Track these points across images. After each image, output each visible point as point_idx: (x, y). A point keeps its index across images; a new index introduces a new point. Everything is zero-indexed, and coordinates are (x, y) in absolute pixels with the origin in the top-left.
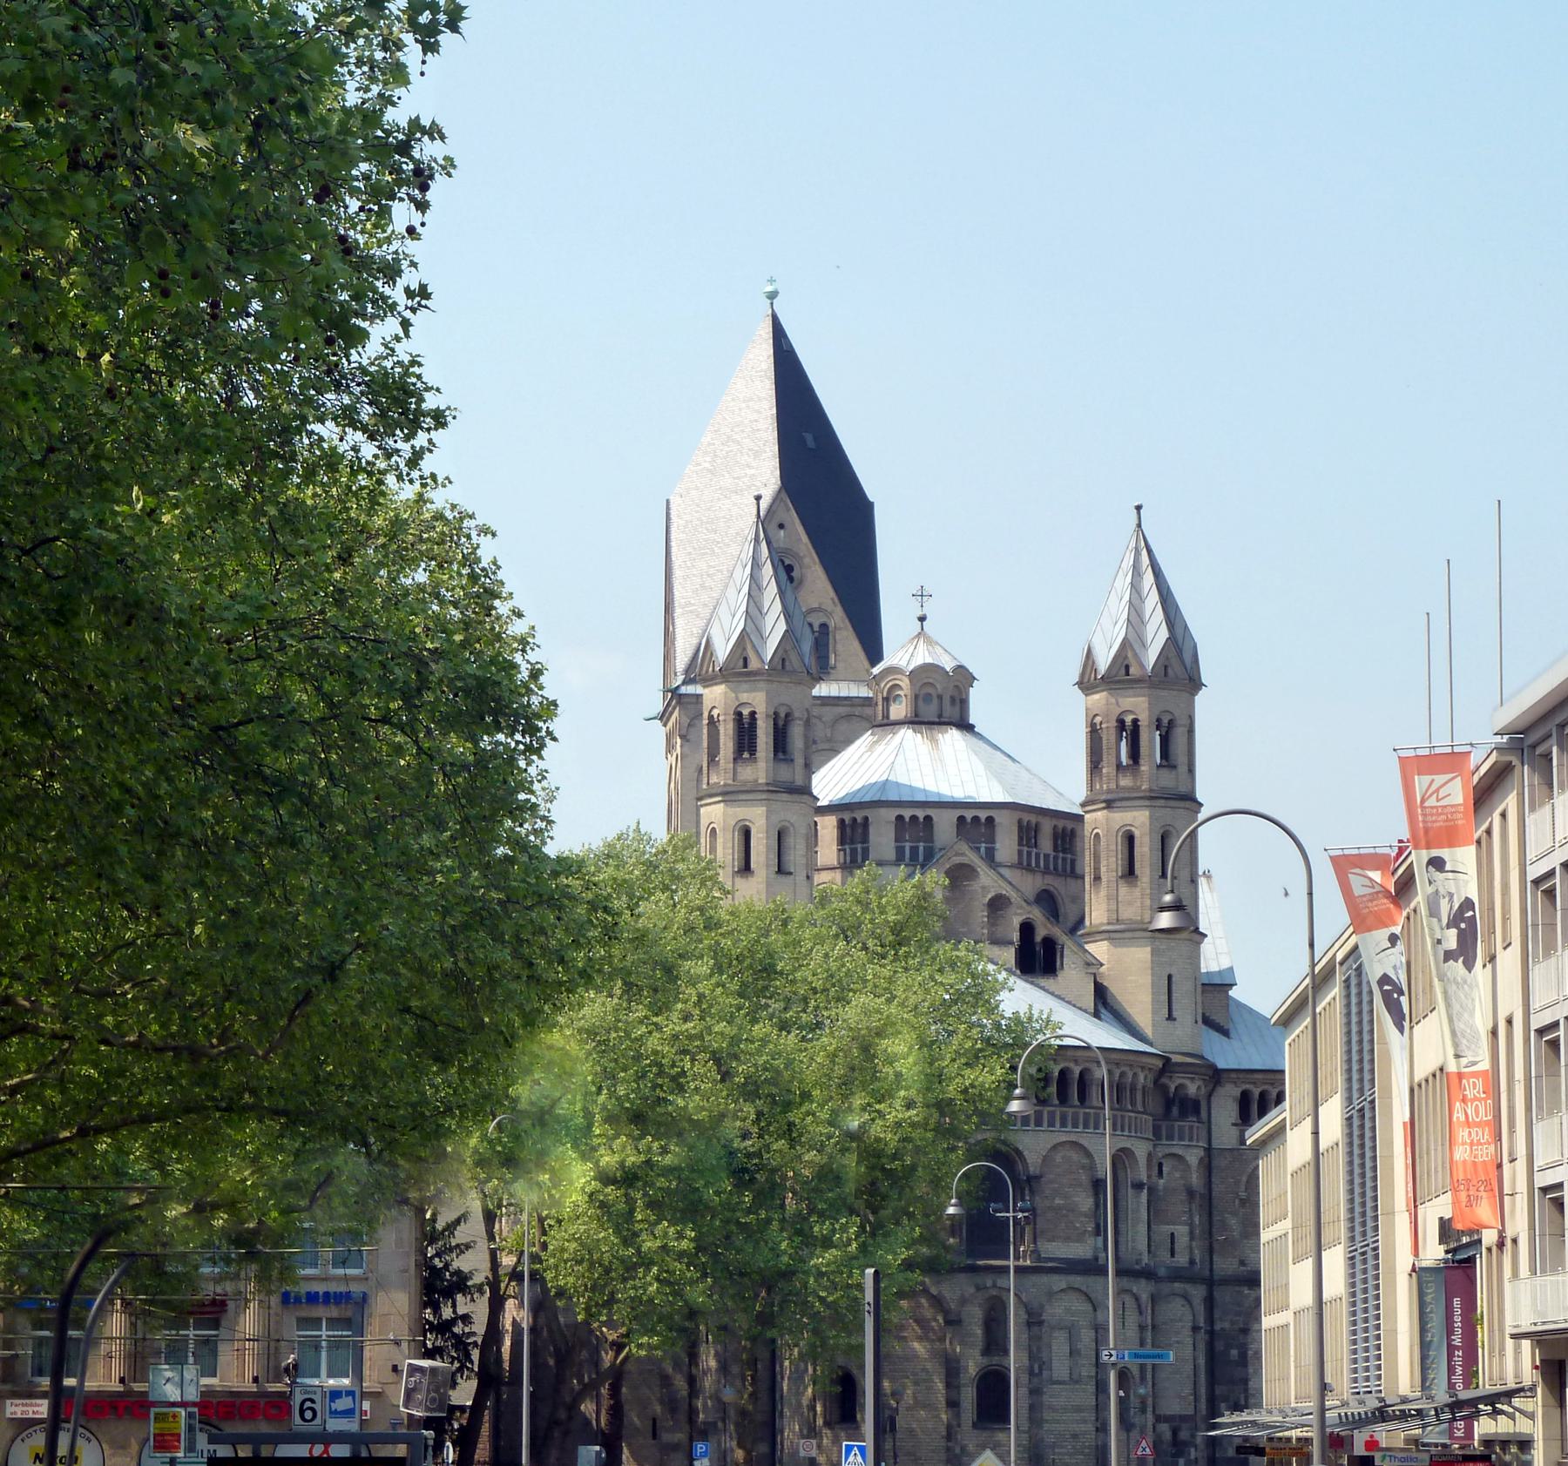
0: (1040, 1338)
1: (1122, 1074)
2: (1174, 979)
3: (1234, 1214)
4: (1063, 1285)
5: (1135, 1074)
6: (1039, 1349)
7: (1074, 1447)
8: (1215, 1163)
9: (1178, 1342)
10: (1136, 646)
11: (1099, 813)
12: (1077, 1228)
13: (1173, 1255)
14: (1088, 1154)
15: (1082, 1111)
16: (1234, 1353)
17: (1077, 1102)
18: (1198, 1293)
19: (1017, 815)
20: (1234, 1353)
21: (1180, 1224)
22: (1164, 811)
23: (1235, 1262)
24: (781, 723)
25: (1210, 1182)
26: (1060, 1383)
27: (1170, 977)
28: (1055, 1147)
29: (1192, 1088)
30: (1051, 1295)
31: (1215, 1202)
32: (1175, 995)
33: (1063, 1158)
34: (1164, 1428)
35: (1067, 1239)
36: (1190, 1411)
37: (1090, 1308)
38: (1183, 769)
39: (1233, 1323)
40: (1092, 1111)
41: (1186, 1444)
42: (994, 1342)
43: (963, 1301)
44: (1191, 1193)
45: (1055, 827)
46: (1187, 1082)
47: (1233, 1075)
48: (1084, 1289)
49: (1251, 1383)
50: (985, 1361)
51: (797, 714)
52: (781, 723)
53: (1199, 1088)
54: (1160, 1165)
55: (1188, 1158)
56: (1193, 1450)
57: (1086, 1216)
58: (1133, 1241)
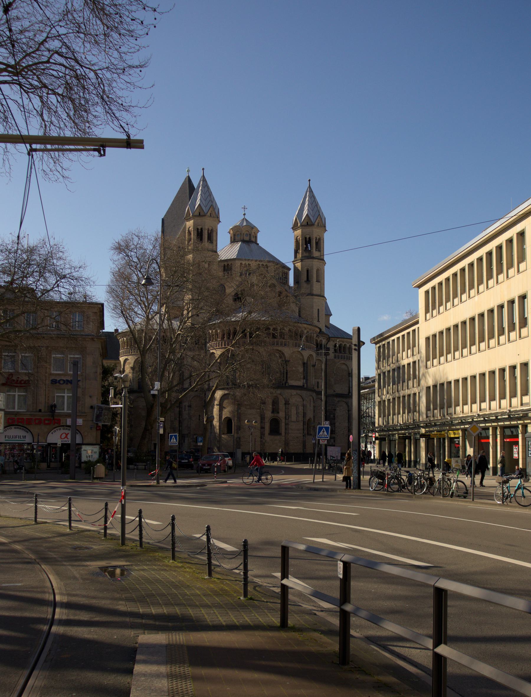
4: (295, 393)
8: (328, 363)
13: (318, 388)
20: (332, 416)
24: (210, 232)
26: (293, 422)
38: (322, 252)
42: (275, 410)
46: (323, 339)
47: (333, 339)
51: (214, 230)
52: (210, 232)
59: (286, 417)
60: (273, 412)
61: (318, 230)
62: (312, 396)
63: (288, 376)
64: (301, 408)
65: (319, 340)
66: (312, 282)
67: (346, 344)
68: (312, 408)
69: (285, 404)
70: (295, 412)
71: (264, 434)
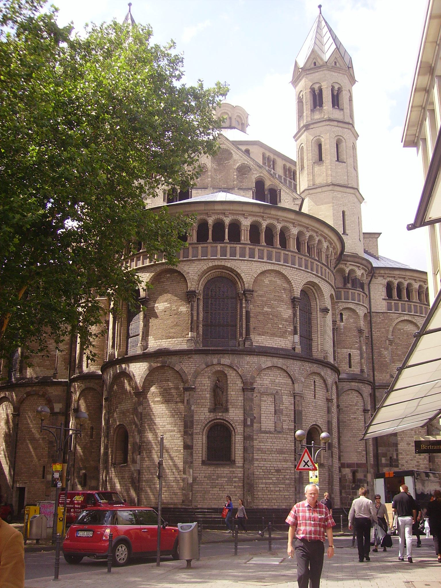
0: (252, 400)
1: (311, 237)
2: (346, 213)
3: (386, 349)
4: (269, 364)
5: (319, 241)
6: (251, 409)
7: (278, 479)
8: (374, 320)
9: (355, 418)
10: (320, 53)
11: (303, 136)
12: (280, 328)
13: (350, 367)
14: (288, 282)
15: (282, 252)
18: (366, 390)
19: (262, 150)
22: (337, 128)
25: (371, 330)
26: (265, 432)
27: (343, 212)
28: (263, 273)
29: (359, 273)
30: (260, 370)
32: (347, 222)
33: (270, 281)
34: (347, 471)
35: (273, 335)
36: (364, 461)
37: (290, 381)
38: (347, 111)
40: (290, 253)
43: (197, 374)
44: (360, 331)
45: (284, 166)
46: (356, 269)
47: (382, 272)
48: (284, 367)
49: (399, 447)
50: (212, 416)
53: (362, 274)
54: (341, 314)
57: (286, 321)
58: (322, 345)
59: (245, 420)
60: (213, 410)
61: (336, 74)
62: (319, 374)
63: (252, 325)
64: (287, 401)
65: (347, 271)
67: (413, 282)
68: (321, 402)
69: (244, 390)
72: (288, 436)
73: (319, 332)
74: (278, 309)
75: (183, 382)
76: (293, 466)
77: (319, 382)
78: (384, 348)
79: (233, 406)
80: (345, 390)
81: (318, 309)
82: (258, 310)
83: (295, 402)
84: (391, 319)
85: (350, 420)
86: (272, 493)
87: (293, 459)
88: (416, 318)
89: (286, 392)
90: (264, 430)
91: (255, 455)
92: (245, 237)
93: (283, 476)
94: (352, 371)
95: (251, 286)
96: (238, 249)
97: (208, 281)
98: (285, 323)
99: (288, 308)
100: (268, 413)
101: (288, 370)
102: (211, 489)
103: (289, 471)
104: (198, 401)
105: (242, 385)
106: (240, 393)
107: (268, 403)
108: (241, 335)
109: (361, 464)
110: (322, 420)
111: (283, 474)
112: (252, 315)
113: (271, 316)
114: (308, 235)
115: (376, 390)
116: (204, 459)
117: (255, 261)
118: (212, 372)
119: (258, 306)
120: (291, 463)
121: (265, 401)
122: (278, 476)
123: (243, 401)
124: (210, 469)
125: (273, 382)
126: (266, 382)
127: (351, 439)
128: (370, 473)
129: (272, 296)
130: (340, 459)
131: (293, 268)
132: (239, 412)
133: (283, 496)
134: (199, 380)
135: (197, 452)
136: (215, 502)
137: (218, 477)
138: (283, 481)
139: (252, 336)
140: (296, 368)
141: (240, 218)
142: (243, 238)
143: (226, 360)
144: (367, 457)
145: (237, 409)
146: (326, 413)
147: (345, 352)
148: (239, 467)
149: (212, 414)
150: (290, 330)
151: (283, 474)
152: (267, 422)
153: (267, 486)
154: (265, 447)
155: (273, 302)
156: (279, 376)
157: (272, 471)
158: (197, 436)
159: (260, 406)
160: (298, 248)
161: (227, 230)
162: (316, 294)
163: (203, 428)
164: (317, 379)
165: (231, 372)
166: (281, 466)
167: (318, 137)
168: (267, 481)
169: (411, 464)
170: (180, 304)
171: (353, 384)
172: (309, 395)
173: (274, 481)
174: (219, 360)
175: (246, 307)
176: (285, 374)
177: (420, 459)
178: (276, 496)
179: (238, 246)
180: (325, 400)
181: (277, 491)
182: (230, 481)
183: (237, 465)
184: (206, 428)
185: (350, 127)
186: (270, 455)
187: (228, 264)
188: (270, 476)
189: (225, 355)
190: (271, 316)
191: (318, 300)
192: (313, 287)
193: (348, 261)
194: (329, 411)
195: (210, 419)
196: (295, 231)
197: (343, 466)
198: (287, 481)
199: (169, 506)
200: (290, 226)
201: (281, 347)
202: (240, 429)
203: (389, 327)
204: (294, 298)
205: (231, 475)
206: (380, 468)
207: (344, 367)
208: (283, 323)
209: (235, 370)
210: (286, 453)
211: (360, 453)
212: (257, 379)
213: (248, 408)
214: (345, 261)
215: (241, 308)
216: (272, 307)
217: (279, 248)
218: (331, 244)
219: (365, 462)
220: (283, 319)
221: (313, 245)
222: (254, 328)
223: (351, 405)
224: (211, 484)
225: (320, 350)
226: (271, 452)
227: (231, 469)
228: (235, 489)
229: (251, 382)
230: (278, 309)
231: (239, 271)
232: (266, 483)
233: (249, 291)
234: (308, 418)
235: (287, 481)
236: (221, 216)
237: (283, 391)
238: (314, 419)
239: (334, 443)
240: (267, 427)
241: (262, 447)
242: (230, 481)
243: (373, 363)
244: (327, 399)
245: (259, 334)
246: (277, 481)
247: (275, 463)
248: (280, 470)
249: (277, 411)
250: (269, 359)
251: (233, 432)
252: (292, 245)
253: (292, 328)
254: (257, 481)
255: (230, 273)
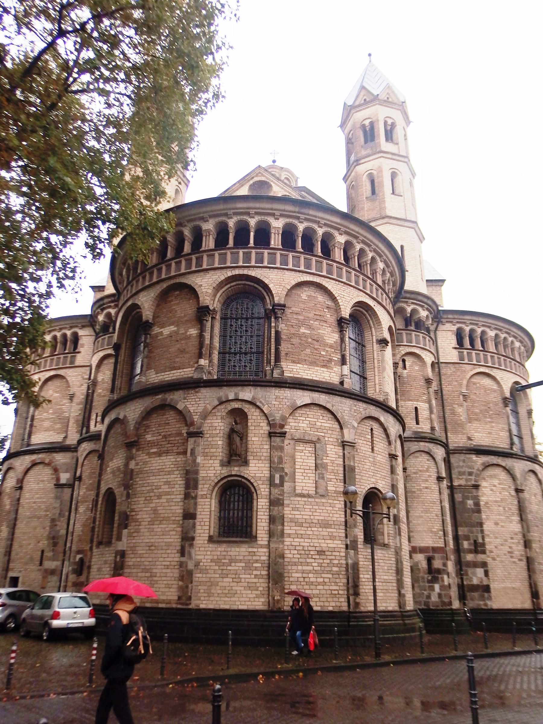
0: (282, 449)
2: (405, 248)
5: (373, 258)
6: (281, 459)
8: (443, 371)
9: (427, 488)
13: (418, 423)
16: (470, 502)
17: (320, 254)
18: (439, 452)
20: (470, 502)
21: (422, 401)
23: (465, 439)
26: (302, 495)
28: (300, 285)
29: (423, 314)
31: (445, 397)
33: (309, 296)
34: (420, 558)
35: (313, 363)
37: (336, 426)
39: (467, 480)
40: (335, 264)
41: (439, 571)
44: (428, 381)
46: (420, 309)
48: (329, 406)
49: (485, 527)
50: (225, 471)
54: (404, 361)
55: (424, 357)
56: (445, 577)
59: (271, 479)
62: (377, 420)
65: (409, 310)
66: (381, 194)
68: (382, 458)
69: (271, 435)
70: (311, 462)
71: (193, 539)
72: (335, 502)
73: (376, 369)
74: (319, 331)
75: (187, 425)
76: (344, 546)
77: (378, 431)
78: (457, 404)
79: (255, 458)
80: (412, 452)
81: (375, 341)
82: (293, 331)
83: (344, 454)
84: (465, 371)
85: (420, 490)
86: (312, 587)
87: (344, 535)
88: (495, 370)
89: (331, 440)
90: (300, 492)
91: (285, 528)
92: (276, 241)
93: (328, 561)
94: (419, 428)
95: (283, 299)
96: (266, 255)
97: (228, 298)
98: (329, 349)
99: (333, 332)
100: (305, 468)
101: (334, 410)
102: (221, 579)
103: (338, 554)
104: (206, 451)
105: (268, 428)
106: (265, 439)
107: (306, 454)
108: (269, 362)
109: (438, 548)
110: (384, 483)
111: (329, 557)
112: (283, 337)
113: (310, 340)
114: (358, 247)
115: (451, 456)
116: (212, 534)
117: (287, 269)
118: (226, 411)
119: (292, 326)
120: (340, 542)
121: (302, 451)
122: (321, 561)
123: (269, 451)
124: (219, 549)
125: (312, 425)
126: (303, 425)
127: (423, 514)
128: (451, 560)
129: (311, 315)
130: (409, 541)
131: (339, 281)
132: (263, 465)
133: (329, 592)
134: (209, 421)
135: (202, 523)
136: (226, 599)
137: (232, 561)
138: (329, 569)
139: (283, 364)
140: (345, 409)
141: (268, 219)
142: (272, 242)
143: (247, 394)
144: (445, 539)
145: (260, 462)
146: (389, 473)
147: (411, 405)
148: (261, 546)
149: (225, 468)
150: (336, 359)
151: (329, 557)
152: (304, 481)
153: (305, 575)
154: (301, 517)
155: (312, 322)
156: (321, 417)
157: (312, 553)
158: (202, 500)
159: (293, 458)
160: (347, 258)
161: (252, 234)
162: (371, 322)
163: (211, 488)
164: (375, 426)
165: (253, 410)
166: (325, 545)
167: (370, 172)
168: (305, 568)
169: (501, 550)
170: (190, 325)
171: (422, 444)
172: (363, 446)
173: (315, 568)
174: (236, 394)
175: (275, 327)
176: (330, 416)
177: (513, 543)
178: (318, 592)
179: (266, 252)
180: (387, 456)
181: (319, 584)
182: (248, 567)
183: (259, 543)
184: (216, 489)
185: (406, 160)
186: (310, 529)
187: (253, 273)
188: (308, 560)
189: (245, 388)
190: (310, 340)
191: (373, 329)
192: (367, 311)
193: (409, 298)
194: (393, 471)
195: (222, 476)
196: (341, 239)
197: (414, 550)
198: (335, 569)
199: (161, 605)
200: (336, 233)
201: (324, 380)
202: (263, 490)
203: (461, 380)
204: (342, 318)
205: (250, 558)
206: (462, 554)
207: (410, 422)
208: (327, 349)
209: (258, 407)
210: (333, 526)
211: (435, 533)
212: (289, 420)
213: (276, 460)
214: (405, 298)
215: (270, 327)
216: (310, 327)
217: (320, 257)
218: (387, 266)
219: (443, 546)
220: (326, 345)
221: (366, 262)
222: (287, 354)
223: (421, 471)
224: (220, 572)
225: (378, 391)
226: (311, 524)
227: (250, 550)
228: (256, 580)
229: (280, 424)
230: (319, 331)
231: (266, 281)
232: (303, 572)
233: (279, 305)
234: (364, 478)
235: (335, 569)
236: (245, 217)
237: (326, 439)
238: (373, 480)
239: (401, 516)
240: (305, 488)
241: (297, 516)
242: (248, 567)
243: (445, 422)
244: (390, 455)
245: (294, 362)
246: (319, 568)
247: (316, 541)
248: (324, 552)
249: (319, 466)
250: (307, 393)
251: (255, 495)
252: (338, 255)
253: (340, 357)
254: (289, 567)
255: (256, 285)
